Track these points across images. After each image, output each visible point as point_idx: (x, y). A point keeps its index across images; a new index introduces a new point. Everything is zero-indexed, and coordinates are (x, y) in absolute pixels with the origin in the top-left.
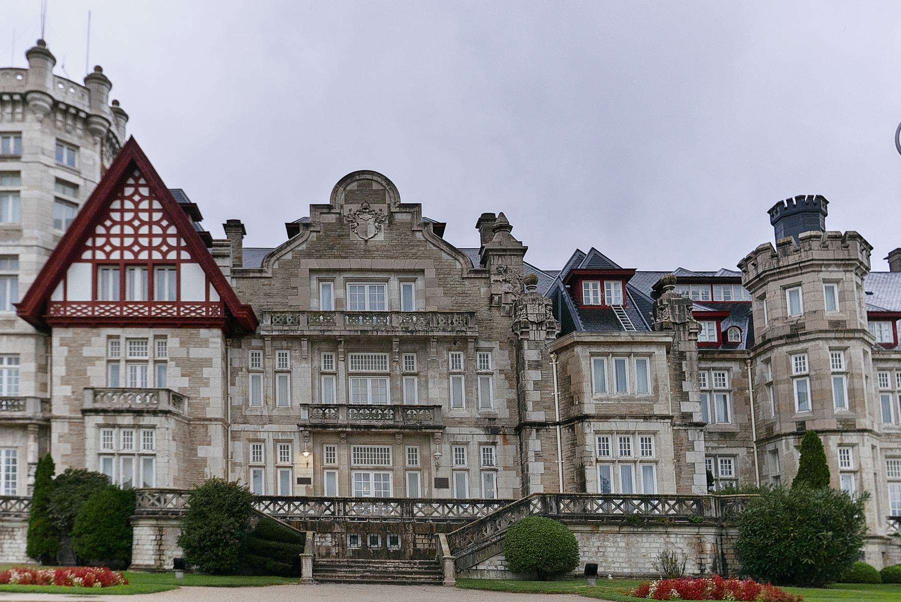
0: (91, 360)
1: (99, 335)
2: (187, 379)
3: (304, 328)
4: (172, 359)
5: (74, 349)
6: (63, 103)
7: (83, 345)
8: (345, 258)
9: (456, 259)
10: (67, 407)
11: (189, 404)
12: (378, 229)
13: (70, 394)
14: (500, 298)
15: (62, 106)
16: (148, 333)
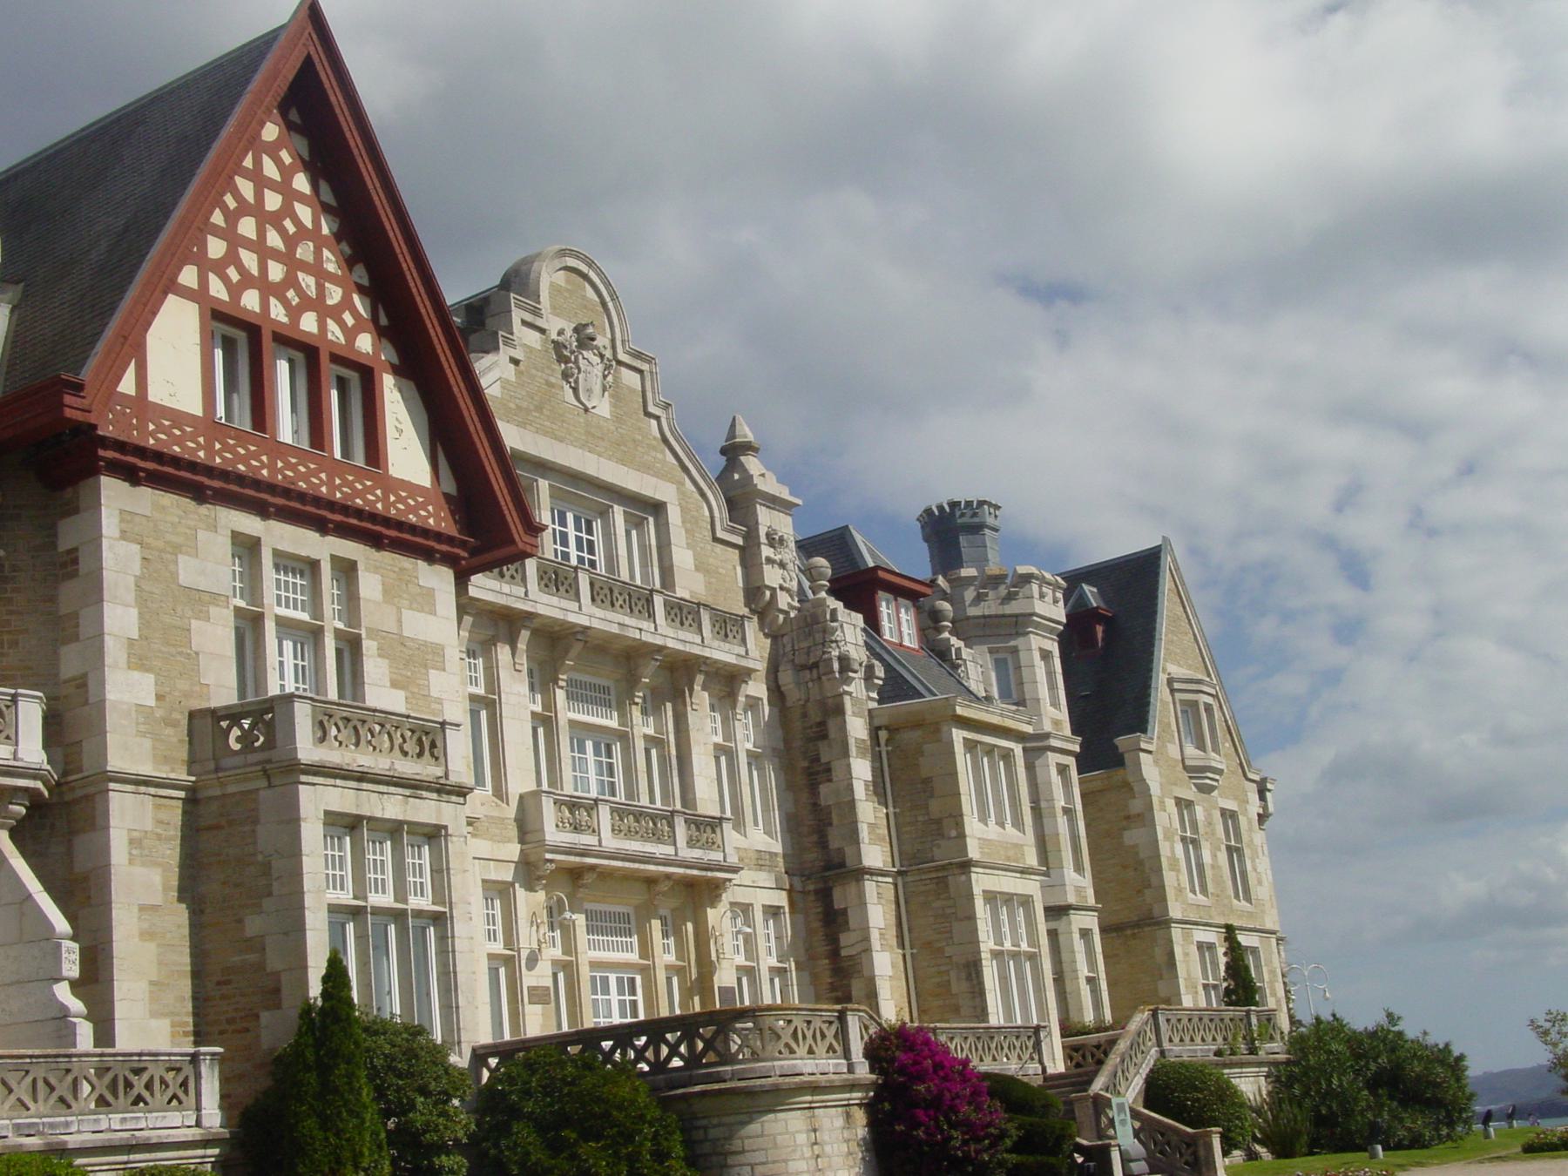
0: (200, 600)
1: (213, 527)
2: (401, 694)
4: (373, 634)
5: (157, 564)
7: (177, 549)
8: (561, 440)
9: (703, 494)
10: (147, 743)
13: (152, 702)
14: (774, 595)
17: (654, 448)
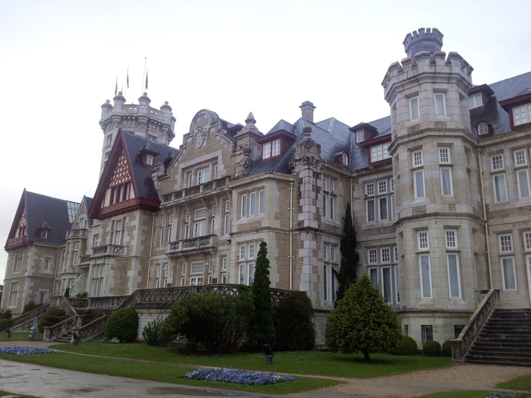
3: (173, 201)
6: (125, 116)
11: (128, 249)
12: (204, 140)
15: (125, 118)
16: (120, 217)
17: (217, 144)
